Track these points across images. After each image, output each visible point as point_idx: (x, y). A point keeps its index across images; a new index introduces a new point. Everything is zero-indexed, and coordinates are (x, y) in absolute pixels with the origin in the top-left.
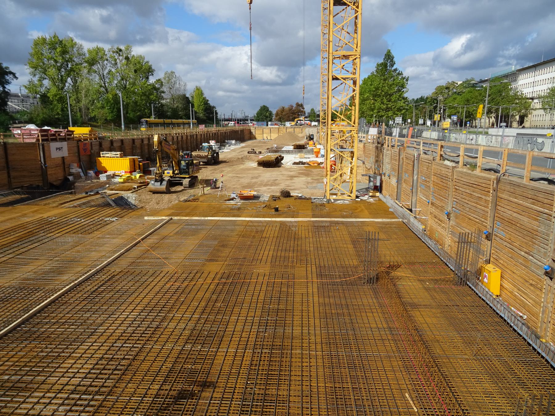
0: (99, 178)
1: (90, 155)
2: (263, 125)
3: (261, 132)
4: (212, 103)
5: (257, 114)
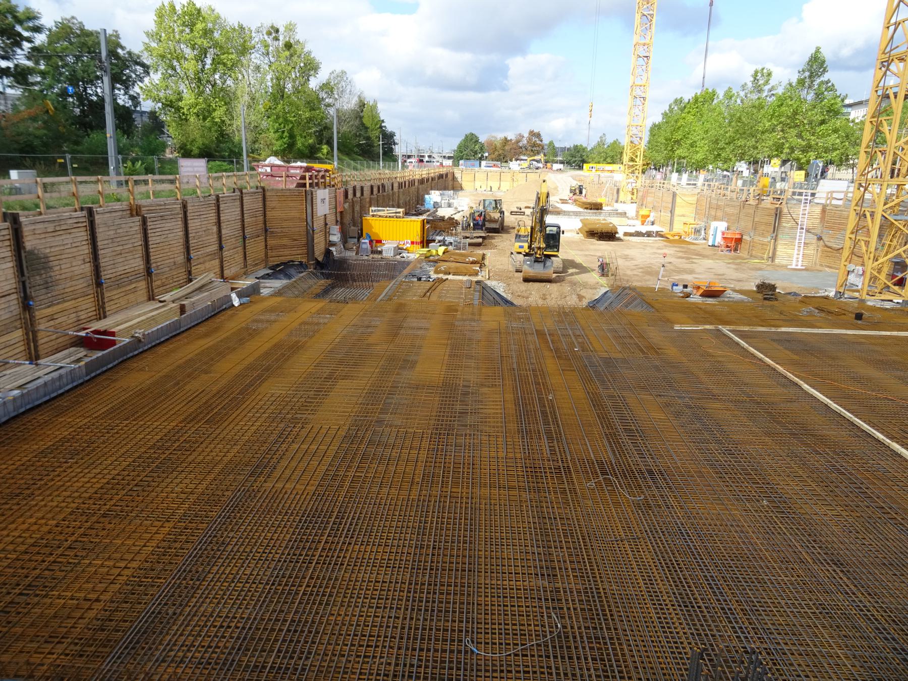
0: (381, 252)
1: (341, 212)
2: (473, 166)
3: (471, 177)
4: (390, 126)
5: (459, 147)
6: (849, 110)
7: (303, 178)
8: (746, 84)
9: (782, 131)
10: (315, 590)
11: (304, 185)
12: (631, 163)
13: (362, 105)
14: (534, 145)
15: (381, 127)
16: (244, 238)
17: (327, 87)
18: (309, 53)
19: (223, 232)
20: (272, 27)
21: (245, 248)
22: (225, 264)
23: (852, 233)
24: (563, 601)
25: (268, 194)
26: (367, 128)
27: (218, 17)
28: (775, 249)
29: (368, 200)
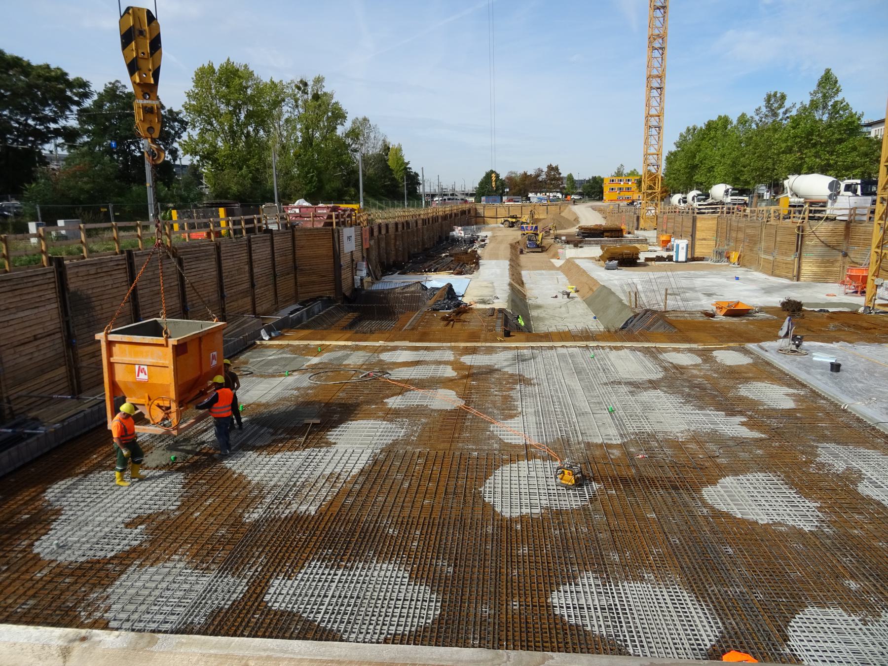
1: (367, 249)
2: (495, 201)
4: (414, 168)
5: (481, 184)
6: (869, 129)
7: (330, 217)
8: (760, 108)
9: (800, 151)
10: (337, 608)
11: (331, 224)
12: (650, 191)
13: (387, 149)
14: (554, 179)
15: (406, 169)
16: (275, 276)
17: (354, 134)
18: (337, 103)
19: (255, 270)
20: (301, 81)
21: (275, 285)
22: (257, 301)
23: (878, 247)
24: (588, 618)
25: (297, 233)
26: (392, 170)
27: (252, 73)
28: (799, 267)
29: (393, 236)
